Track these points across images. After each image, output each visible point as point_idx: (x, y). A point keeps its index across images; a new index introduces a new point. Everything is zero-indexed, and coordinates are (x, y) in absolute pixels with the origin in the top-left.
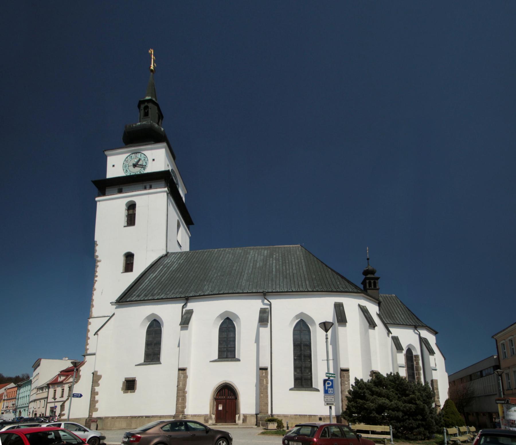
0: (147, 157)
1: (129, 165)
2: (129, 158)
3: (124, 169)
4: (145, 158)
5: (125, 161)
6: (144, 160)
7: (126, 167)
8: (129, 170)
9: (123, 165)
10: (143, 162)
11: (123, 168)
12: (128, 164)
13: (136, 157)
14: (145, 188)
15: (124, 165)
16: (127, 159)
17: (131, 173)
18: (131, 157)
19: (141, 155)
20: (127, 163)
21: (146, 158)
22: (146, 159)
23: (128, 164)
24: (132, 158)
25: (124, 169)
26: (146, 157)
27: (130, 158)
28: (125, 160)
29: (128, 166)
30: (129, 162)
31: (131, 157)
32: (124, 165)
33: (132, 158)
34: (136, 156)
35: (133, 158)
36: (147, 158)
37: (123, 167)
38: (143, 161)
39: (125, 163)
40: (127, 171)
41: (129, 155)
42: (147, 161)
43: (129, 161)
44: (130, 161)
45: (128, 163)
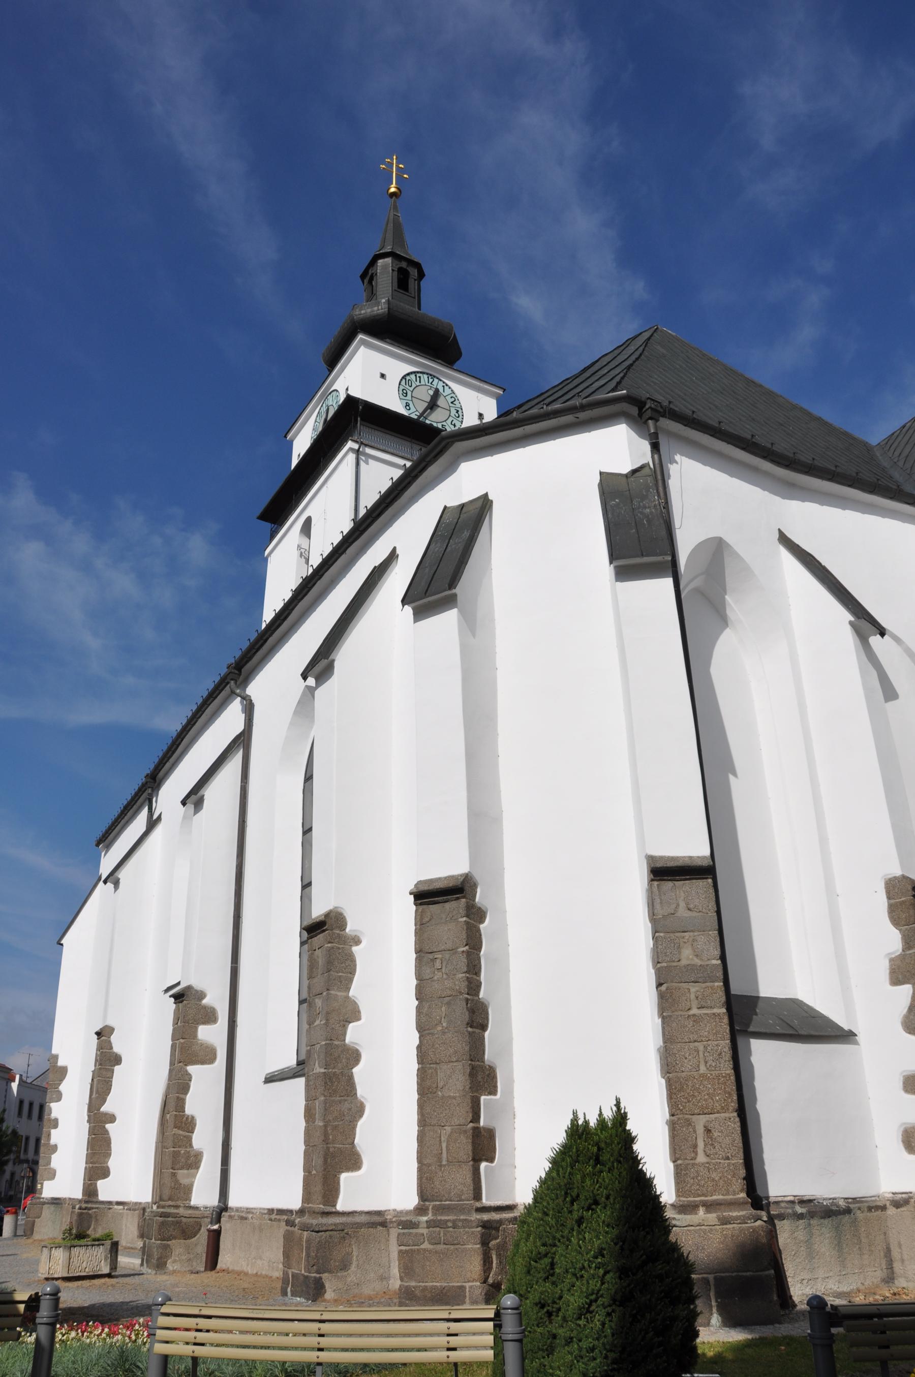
2: (413, 377)
5: (404, 380)
6: (452, 403)
7: (406, 393)
13: (430, 385)
15: (402, 387)
18: (420, 377)
23: (412, 392)
29: (412, 397)
31: (418, 379)
33: (420, 382)
35: (423, 383)
41: (414, 372)
43: (414, 386)
44: (417, 386)
45: (411, 389)
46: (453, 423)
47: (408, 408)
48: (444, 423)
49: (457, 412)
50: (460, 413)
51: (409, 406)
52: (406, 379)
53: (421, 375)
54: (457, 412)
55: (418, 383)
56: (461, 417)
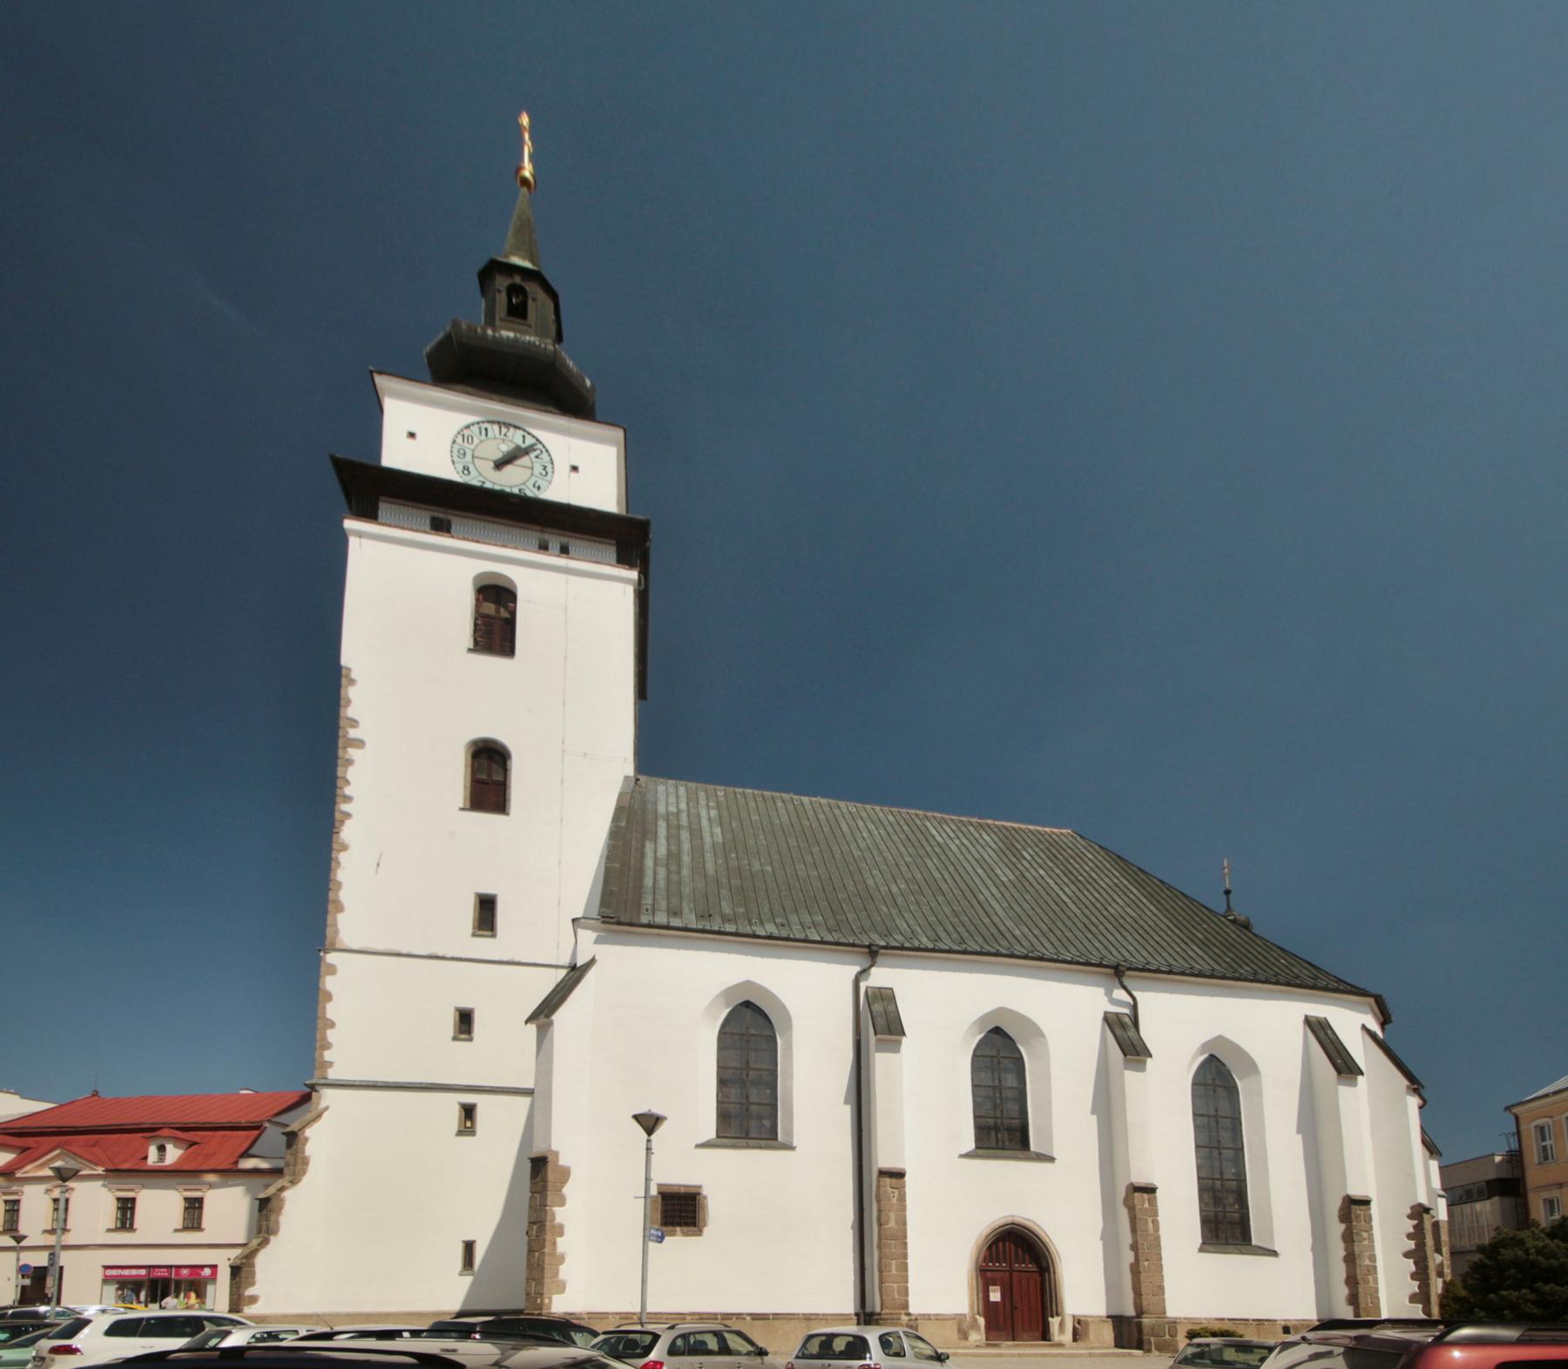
0: (547, 451)
2: (475, 429)
4: (542, 452)
5: (460, 437)
7: (465, 454)
8: (476, 468)
10: (532, 463)
11: (452, 456)
12: (473, 450)
13: (502, 436)
14: (544, 547)
15: (456, 447)
16: (466, 432)
17: (484, 483)
18: (486, 430)
19: (524, 437)
21: (545, 453)
24: (487, 435)
25: (456, 459)
26: (544, 450)
27: (480, 433)
28: (459, 433)
29: (473, 457)
31: (484, 432)
32: (456, 447)
33: (487, 435)
34: (505, 435)
36: (549, 455)
41: (478, 423)
43: (476, 441)
44: (481, 441)
45: (472, 447)
46: (537, 485)
48: (523, 487)
49: (545, 468)
50: (549, 469)
51: (468, 470)
52: (463, 436)
53: (488, 426)
54: (545, 468)
56: (550, 474)
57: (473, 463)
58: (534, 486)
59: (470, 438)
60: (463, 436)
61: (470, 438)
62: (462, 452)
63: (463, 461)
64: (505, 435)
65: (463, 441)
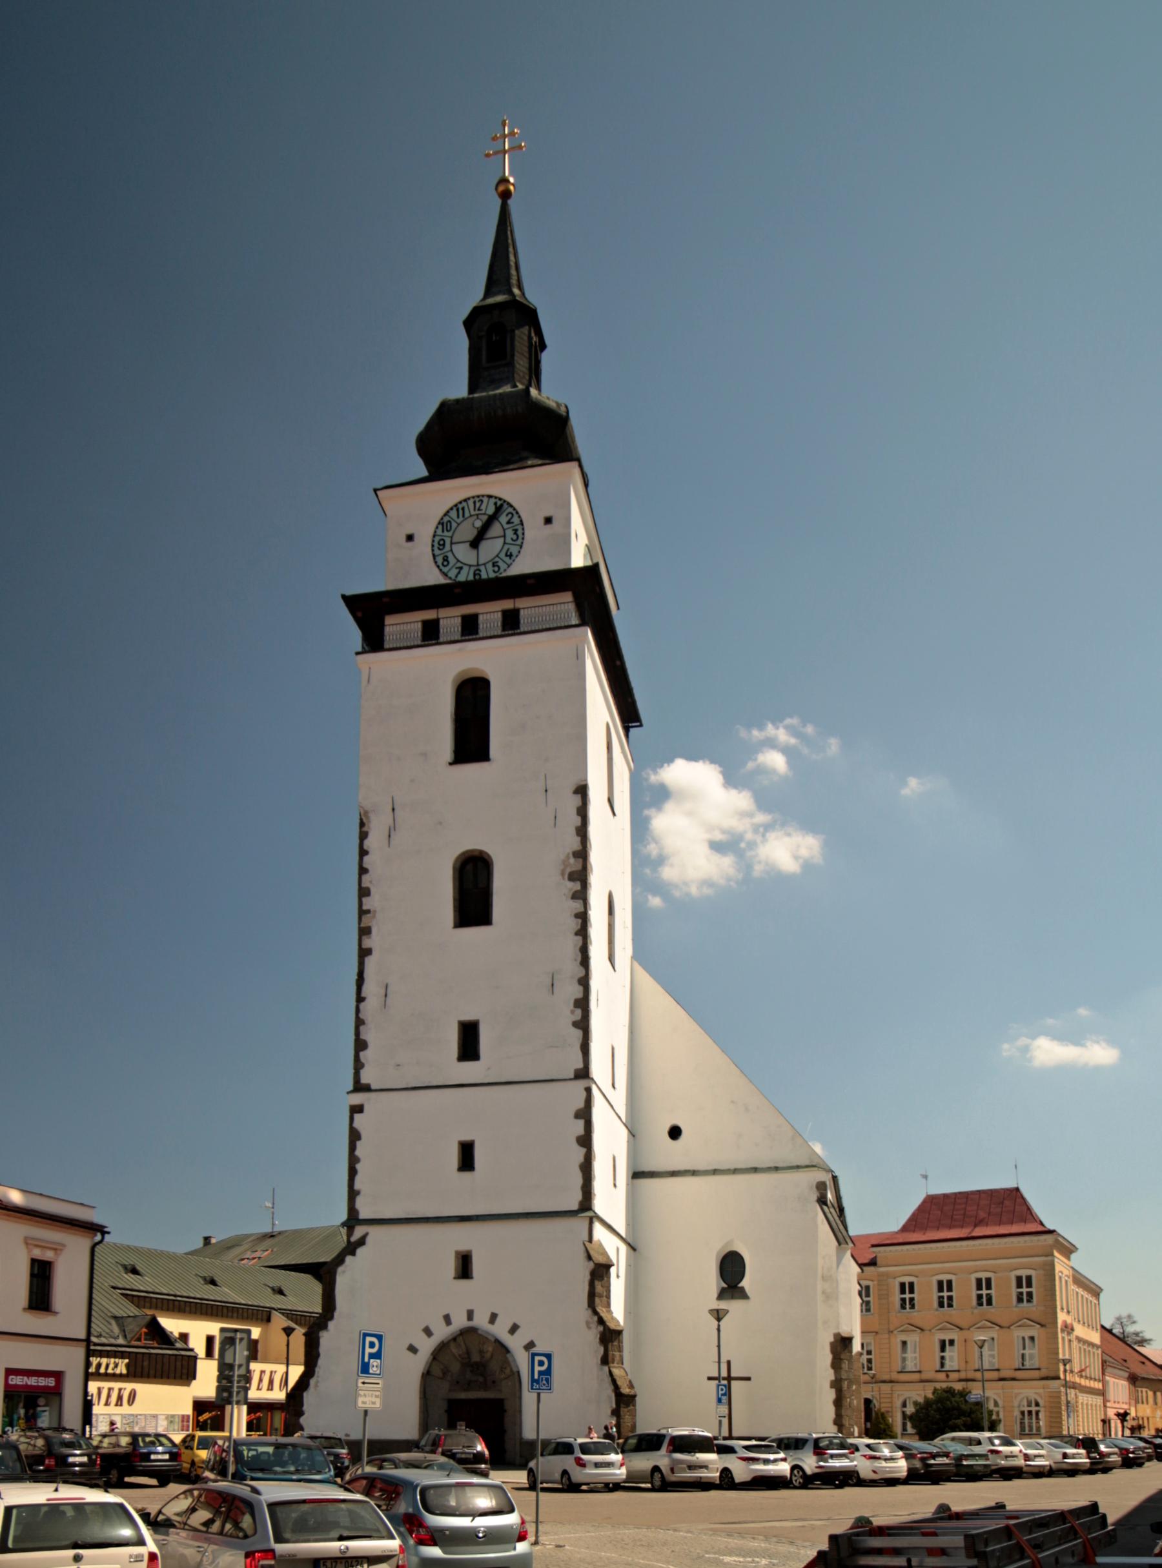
0: (517, 513)
1: (454, 540)
3: (437, 552)
4: (513, 515)
5: (440, 527)
6: (509, 522)
7: (444, 545)
8: (454, 556)
9: (433, 541)
10: (504, 530)
15: (437, 539)
18: (463, 509)
20: (446, 533)
21: (516, 516)
22: (516, 520)
23: (452, 537)
24: (463, 516)
25: (437, 552)
26: (514, 512)
27: (458, 517)
28: (439, 523)
29: (452, 543)
30: (456, 529)
31: (461, 512)
33: (463, 516)
35: (467, 514)
36: (519, 517)
37: (433, 546)
38: (506, 526)
39: (439, 532)
40: (446, 559)
42: (519, 527)
43: (454, 525)
44: (458, 524)
46: (509, 554)
47: (445, 563)
48: (497, 559)
50: (520, 533)
53: (464, 504)
55: (461, 518)
56: (521, 536)
57: (451, 550)
58: (506, 555)
59: (449, 524)
60: (443, 524)
61: (449, 524)
62: (442, 542)
63: (442, 552)
64: (479, 510)
65: (443, 531)
